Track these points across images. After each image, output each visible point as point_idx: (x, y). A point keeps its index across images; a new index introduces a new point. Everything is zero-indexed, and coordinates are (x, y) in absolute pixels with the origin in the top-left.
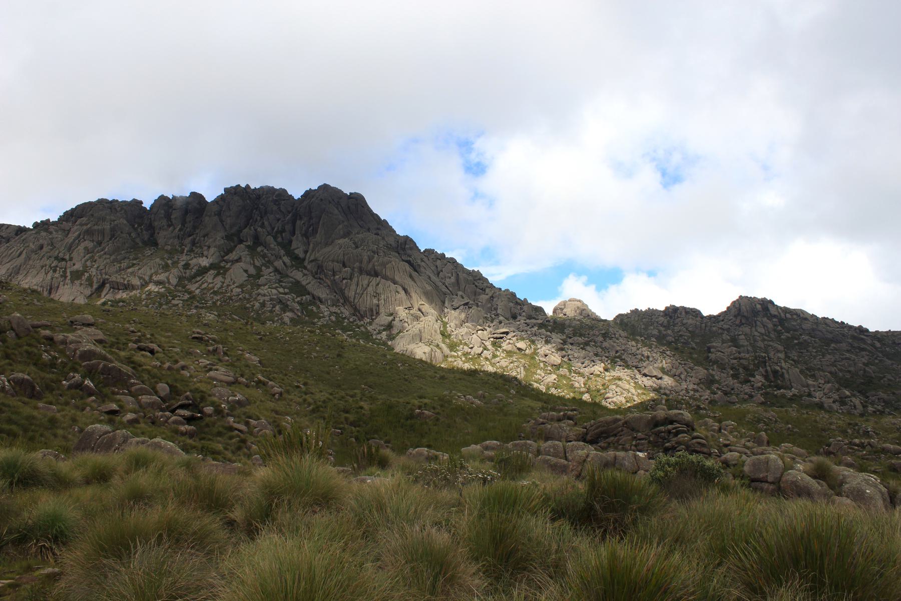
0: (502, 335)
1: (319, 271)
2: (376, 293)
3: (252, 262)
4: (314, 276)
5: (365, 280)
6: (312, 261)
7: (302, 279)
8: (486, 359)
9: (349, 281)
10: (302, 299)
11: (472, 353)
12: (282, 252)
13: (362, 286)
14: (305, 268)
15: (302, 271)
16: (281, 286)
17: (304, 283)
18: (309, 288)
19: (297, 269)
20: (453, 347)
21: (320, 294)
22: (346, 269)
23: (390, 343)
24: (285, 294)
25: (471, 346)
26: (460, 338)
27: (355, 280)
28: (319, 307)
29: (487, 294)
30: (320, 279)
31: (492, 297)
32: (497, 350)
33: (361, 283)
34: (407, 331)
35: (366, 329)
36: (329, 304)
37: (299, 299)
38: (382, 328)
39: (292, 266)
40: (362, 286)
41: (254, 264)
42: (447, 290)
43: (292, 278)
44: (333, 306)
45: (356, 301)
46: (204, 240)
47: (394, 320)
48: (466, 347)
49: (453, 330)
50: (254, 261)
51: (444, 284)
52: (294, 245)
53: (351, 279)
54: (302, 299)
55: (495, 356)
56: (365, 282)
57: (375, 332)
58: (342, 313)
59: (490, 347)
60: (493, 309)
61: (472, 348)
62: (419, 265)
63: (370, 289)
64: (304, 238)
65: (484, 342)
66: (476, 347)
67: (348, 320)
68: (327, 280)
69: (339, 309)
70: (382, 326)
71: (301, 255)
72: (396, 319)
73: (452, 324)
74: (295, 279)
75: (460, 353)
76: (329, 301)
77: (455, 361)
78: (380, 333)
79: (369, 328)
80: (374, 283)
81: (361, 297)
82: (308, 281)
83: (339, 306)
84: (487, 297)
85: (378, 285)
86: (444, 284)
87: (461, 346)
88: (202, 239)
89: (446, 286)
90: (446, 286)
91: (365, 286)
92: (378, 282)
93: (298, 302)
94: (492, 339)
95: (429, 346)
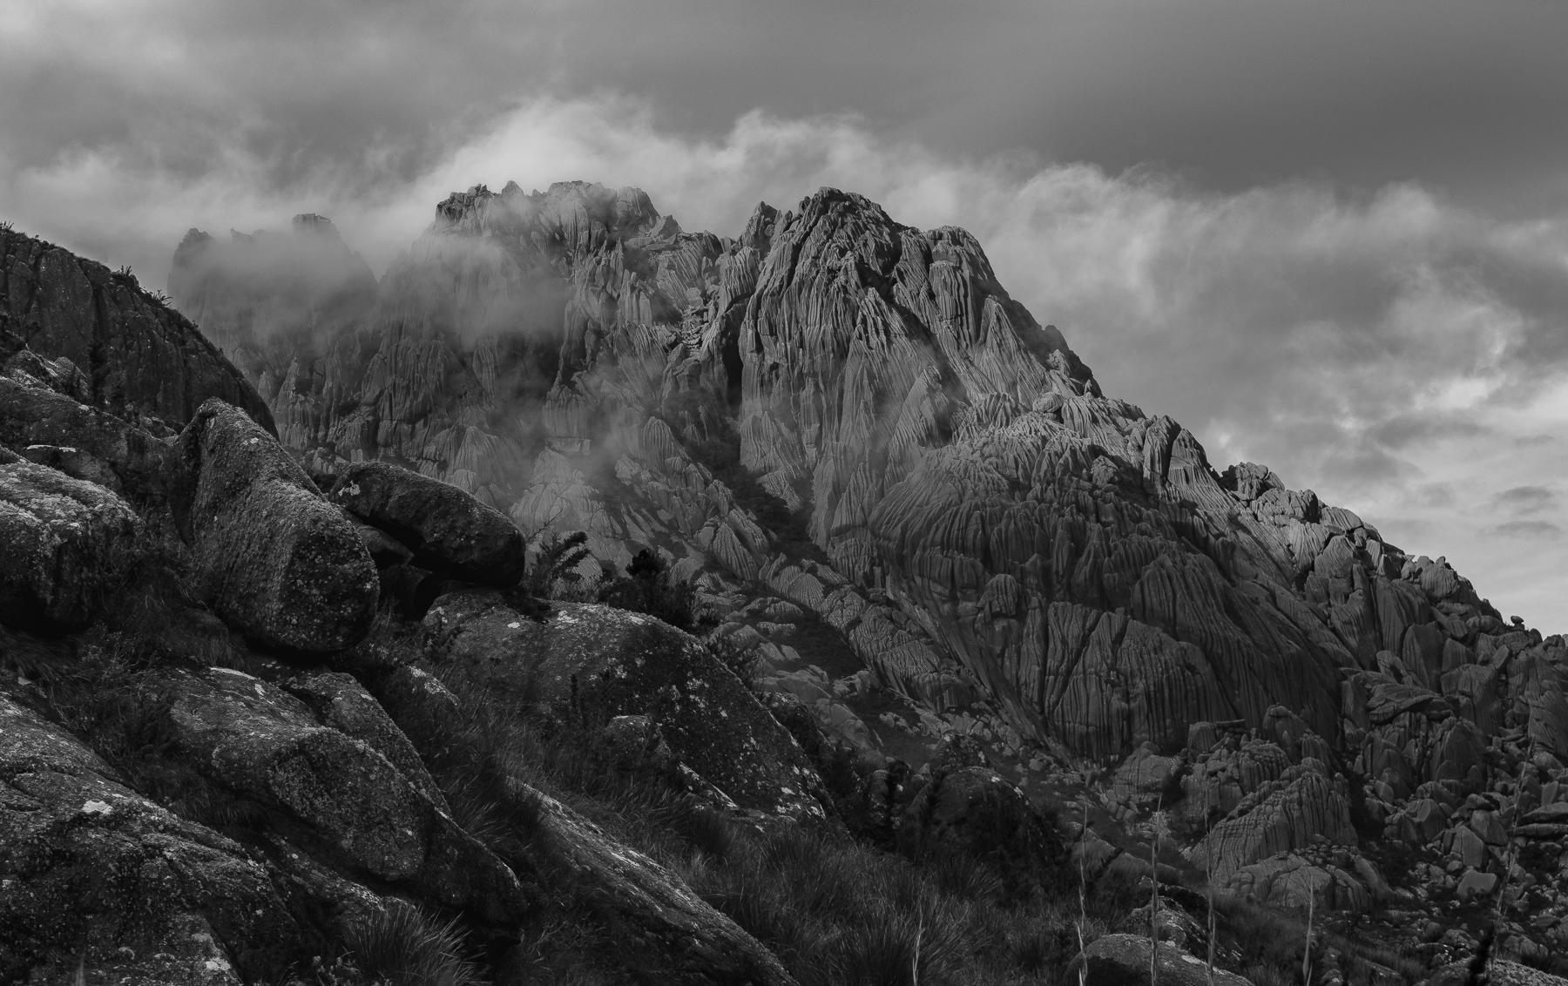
0: (1553, 827)
1: (878, 570)
2: (1118, 673)
3: (618, 529)
4: (864, 594)
5: (1068, 622)
6: (841, 532)
7: (825, 606)
8: (1512, 914)
9: (1013, 622)
10: (852, 686)
11: (1462, 890)
12: (722, 492)
13: (1064, 642)
14: (823, 558)
15: (813, 570)
16: (766, 632)
17: (838, 620)
18: (862, 638)
19: (793, 560)
20: (1396, 869)
21: (912, 669)
22: (1000, 577)
23: (1186, 852)
24: (792, 666)
25: (1455, 865)
26: (1414, 836)
27: (1034, 621)
28: (917, 717)
29: (1485, 663)
30: (889, 603)
31: (1504, 670)
32: (1541, 881)
33: (1057, 633)
34: (1242, 813)
35: (1097, 800)
36: (947, 705)
37: (840, 686)
38: (1148, 798)
39: (774, 549)
40: (1064, 642)
41: (626, 536)
42: (1343, 650)
43: (783, 597)
44: (959, 712)
45: (1050, 699)
46: (412, 435)
47: (1185, 770)
48: (1436, 869)
49: (1388, 805)
50: (623, 525)
51: (1325, 620)
52: (751, 459)
53: (1021, 615)
54: (852, 686)
55: (1537, 903)
56: (1074, 630)
57: (1129, 814)
58: (996, 738)
59: (1515, 869)
60: (1508, 720)
61: (1458, 874)
62: (1231, 548)
63: (1093, 656)
64: (784, 430)
65: (1497, 851)
66: (1470, 870)
67: (1025, 765)
68: (918, 612)
69: (987, 725)
70: (1146, 789)
71: (793, 502)
72: (1198, 767)
73: (1382, 785)
74: (800, 605)
75: (1422, 892)
76: (946, 694)
77: (1414, 918)
78: (1144, 814)
79: (1104, 798)
80: (1103, 632)
81: (1065, 684)
82: (849, 614)
83: (981, 712)
84: (1487, 673)
85: (1118, 639)
86: (1325, 620)
87: (1423, 866)
88: (406, 427)
89: (1334, 630)
90: (1334, 630)
91: (1072, 644)
92: (1116, 628)
93: (842, 698)
94: (1520, 842)
95: (1322, 866)
